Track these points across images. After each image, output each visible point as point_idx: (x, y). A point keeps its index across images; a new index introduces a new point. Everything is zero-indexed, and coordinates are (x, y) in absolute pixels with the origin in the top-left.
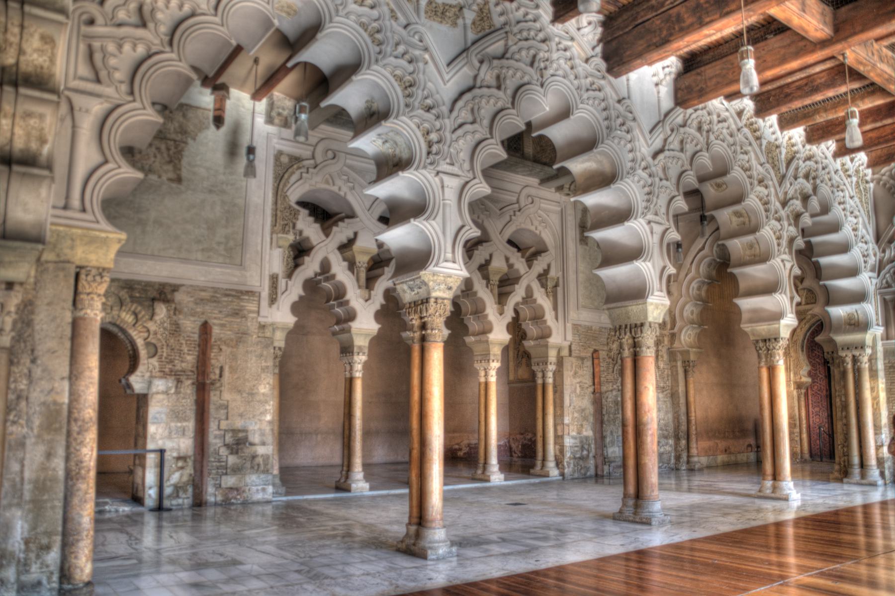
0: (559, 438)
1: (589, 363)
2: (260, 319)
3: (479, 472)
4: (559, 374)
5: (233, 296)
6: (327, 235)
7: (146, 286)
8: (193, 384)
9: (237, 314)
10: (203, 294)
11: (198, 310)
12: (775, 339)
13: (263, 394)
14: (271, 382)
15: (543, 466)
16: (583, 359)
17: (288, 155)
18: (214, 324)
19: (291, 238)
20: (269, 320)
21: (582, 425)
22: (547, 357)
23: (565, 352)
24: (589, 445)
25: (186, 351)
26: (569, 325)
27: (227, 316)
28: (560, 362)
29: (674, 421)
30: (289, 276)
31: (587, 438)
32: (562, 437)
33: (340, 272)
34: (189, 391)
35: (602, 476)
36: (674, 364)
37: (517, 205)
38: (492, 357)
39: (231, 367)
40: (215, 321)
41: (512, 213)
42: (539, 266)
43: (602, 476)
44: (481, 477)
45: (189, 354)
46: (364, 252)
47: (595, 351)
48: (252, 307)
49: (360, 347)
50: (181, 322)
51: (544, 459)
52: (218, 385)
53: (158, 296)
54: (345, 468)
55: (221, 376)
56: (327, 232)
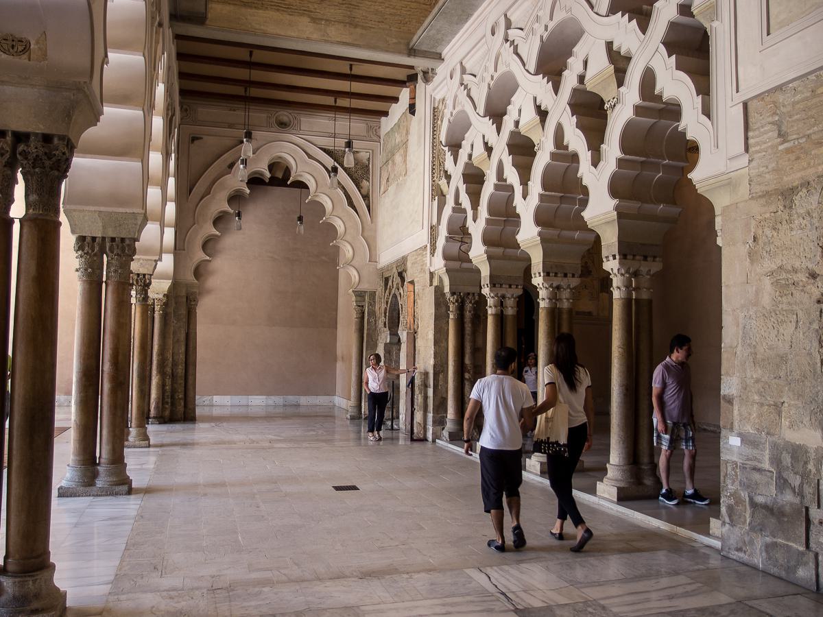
21: (778, 408)
38: (604, 253)
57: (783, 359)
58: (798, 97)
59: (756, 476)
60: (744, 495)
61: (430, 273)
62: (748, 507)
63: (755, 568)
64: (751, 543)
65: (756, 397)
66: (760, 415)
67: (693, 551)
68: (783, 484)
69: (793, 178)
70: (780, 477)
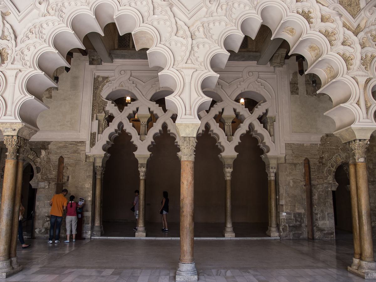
5: (74, 144)
7: (36, 143)
8: (55, 184)
9: (76, 152)
10: (60, 144)
11: (58, 152)
12: (354, 141)
13: (87, 188)
14: (91, 182)
16: (295, 165)
17: (102, 77)
18: (65, 157)
21: (295, 206)
23: (283, 161)
25: (52, 170)
26: (283, 145)
27: (71, 153)
31: (300, 214)
32: (279, 212)
33: (129, 127)
34: (53, 187)
37: (242, 78)
38: (226, 166)
39: (72, 176)
40: (65, 156)
41: (239, 84)
42: (259, 111)
45: (53, 171)
46: (229, 118)
48: (82, 148)
49: (142, 164)
50: (50, 157)
52: (67, 184)
53: (42, 147)
55: (68, 180)
56: (121, 109)
57: (295, 196)
58: (296, 147)
59: (290, 220)
60: (287, 225)
61: (86, 155)
62: (288, 227)
63: (290, 239)
64: (289, 235)
65: (290, 204)
66: (291, 208)
67: (269, 242)
68: (296, 221)
69: (295, 162)
70: (296, 219)
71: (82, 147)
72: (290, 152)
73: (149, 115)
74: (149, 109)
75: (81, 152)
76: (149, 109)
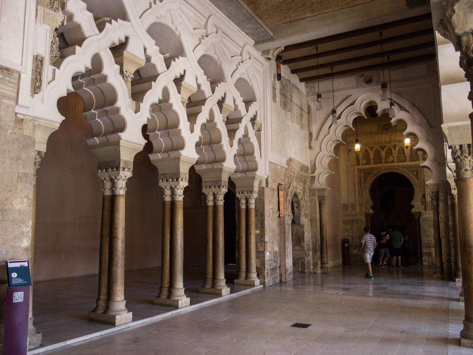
0: (261, 254)
1: (276, 194)
2: (18, 109)
3: (208, 286)
4: (260, 202)
6: (101, 27)
13: (19, 211)
15: (247, 277)
16: (273, 190)
19: (59, 18)
20: (30, 113)
22: (253, 187)
23: (264, 184)
24: (277, 258)
28: (261, 192)
29: (312, 239)
30: (57, 63)
31: (276, 252)
32: (263, 252)
35: (285, 283)
36: (313, 198)
43: (285, 283)
44: (212, 291)
47: (279, 185)
49: (126, 162)
51: (248, 270)
54: (103, 297)
59: (271, 261)
71: (5, 87)
72: (271, 173)
73: (143, 63)
74: (145, 50)
75: (4, 101)
76: (145, 50)
